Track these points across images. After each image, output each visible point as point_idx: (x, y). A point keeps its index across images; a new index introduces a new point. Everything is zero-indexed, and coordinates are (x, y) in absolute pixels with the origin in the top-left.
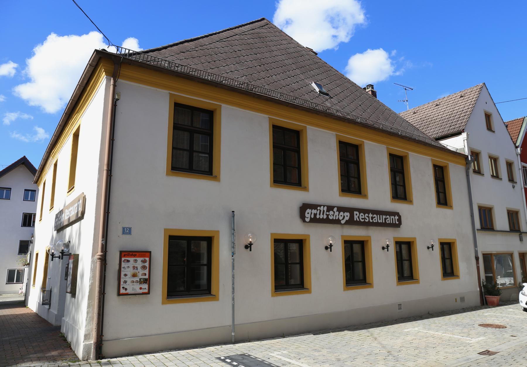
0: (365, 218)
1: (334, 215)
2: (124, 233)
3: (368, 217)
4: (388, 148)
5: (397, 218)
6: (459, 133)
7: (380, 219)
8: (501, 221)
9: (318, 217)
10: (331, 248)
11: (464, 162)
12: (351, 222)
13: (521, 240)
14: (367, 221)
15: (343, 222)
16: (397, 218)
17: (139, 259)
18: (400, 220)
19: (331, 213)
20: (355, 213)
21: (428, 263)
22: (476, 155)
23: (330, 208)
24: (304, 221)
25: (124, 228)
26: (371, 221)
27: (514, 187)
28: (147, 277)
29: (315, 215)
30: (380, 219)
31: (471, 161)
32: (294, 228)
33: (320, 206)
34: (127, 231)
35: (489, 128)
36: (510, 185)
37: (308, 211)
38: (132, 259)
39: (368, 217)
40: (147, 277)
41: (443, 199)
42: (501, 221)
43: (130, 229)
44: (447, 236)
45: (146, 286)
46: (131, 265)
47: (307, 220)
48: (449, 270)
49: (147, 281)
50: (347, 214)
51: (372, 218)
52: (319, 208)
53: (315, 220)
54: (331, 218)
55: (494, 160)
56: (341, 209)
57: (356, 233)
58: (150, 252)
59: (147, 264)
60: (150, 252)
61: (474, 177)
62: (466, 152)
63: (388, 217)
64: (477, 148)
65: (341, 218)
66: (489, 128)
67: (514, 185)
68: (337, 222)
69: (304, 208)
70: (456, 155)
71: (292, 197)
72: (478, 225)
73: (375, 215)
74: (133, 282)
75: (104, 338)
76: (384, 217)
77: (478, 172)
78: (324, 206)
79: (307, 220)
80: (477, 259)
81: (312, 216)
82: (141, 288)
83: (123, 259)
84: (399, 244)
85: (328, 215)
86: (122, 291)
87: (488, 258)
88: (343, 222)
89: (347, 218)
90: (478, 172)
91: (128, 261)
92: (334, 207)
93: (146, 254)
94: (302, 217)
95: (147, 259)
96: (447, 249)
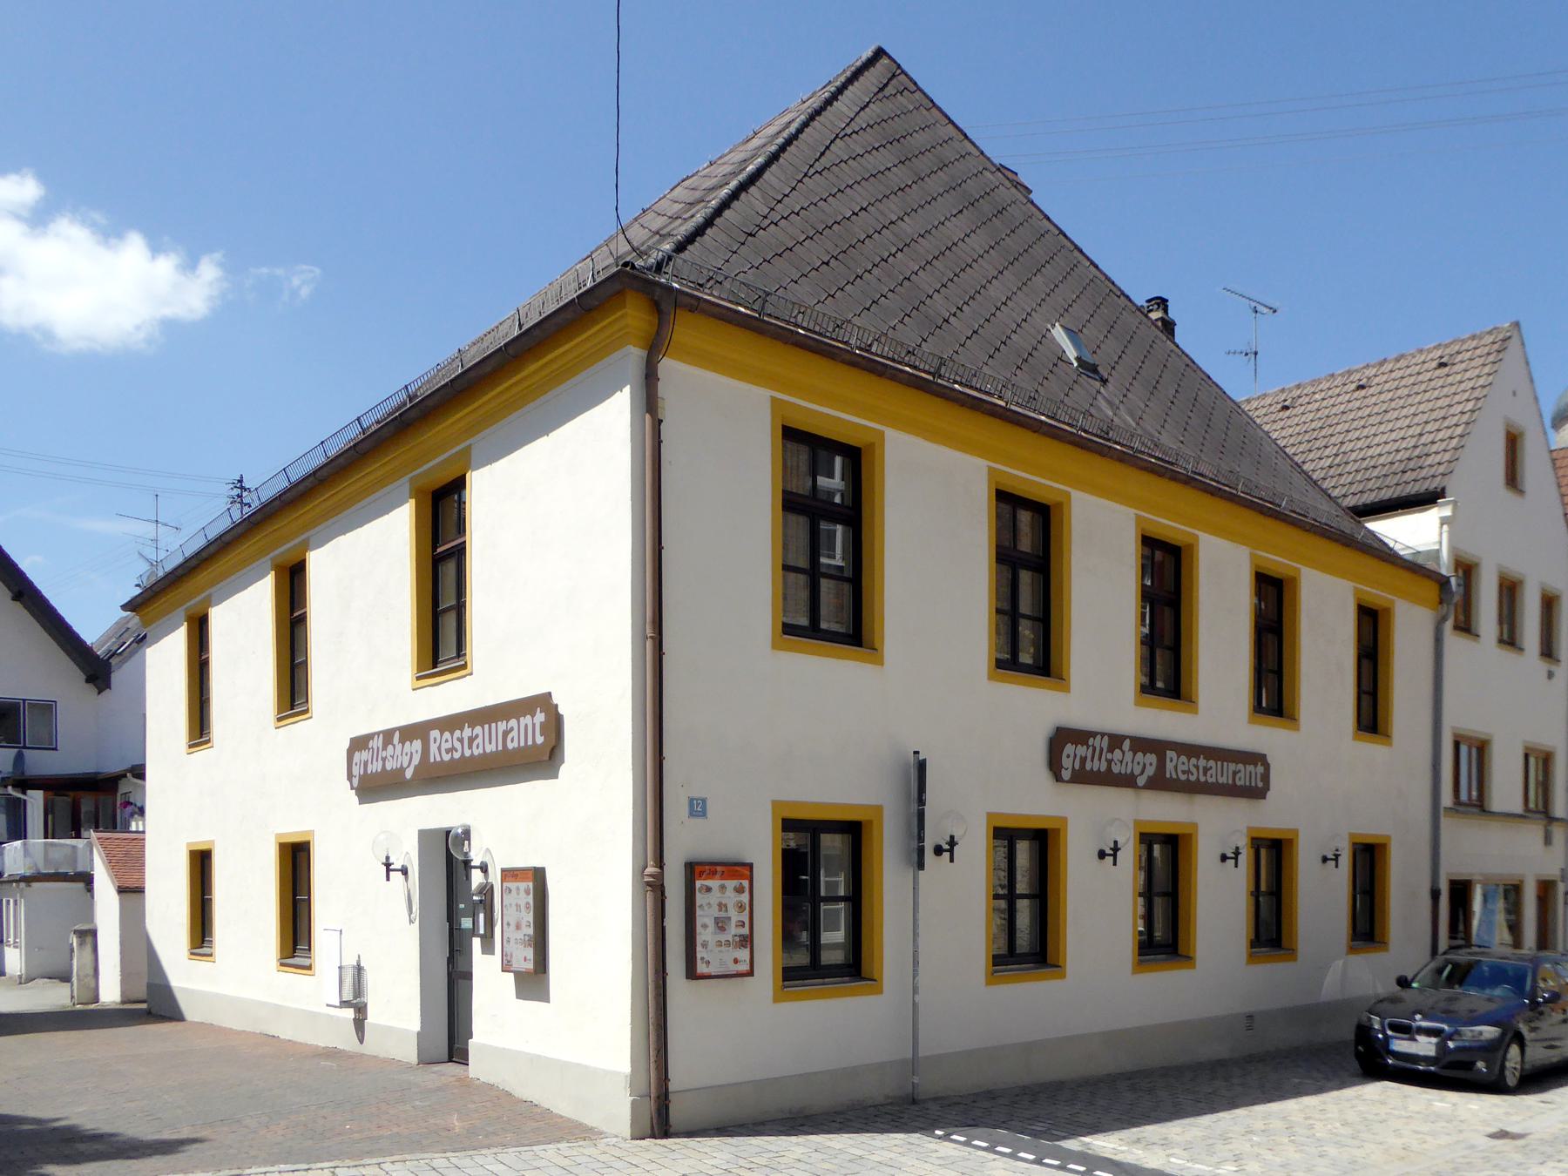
0: (1188, 772)
1: (1124, 762)
2: (693, 813)
3: (1197, 767)
4: (1252, 556)
5: (1260, 769)
6: (1426, 500)
7: (1220, 773)
8: (1506, 789)
9: (1088, 766)
10: (1115, 856)
11: (1431, 590)
12: (1160, 783)
13: (1548, 840)
14: (1193, 778)
15: (1141, 781)
16: (1260, 769)
17: (731, 884)
18: (1266, 777)
19: (1117, 754)
20: (1170, 754)
21: (1320, 895)
22: (1467, 570)
23: (1116, 741)
24: (1058, 778)
25: (691, 800)
26: (1202, 779)
27: (1550, 675)
28: (746, 931)
29: (1083, 760)
30: (1220, 773)
31: (1451, 590)
32: (1036, 798)
33: (1093, 734)
34: (698, 808)
35: (1513, 479)
36: (1542, 666)
37: (1069, 749)
38: (714, 883)
39: (1197, 767)
40: (746, 931)
41: (1371, 717)
42: (1506, 789)
43: (704, 801)
44: (1370, 829)
45: (744, 954)
46: (716, 896)
47: (1066, 775)
48: (1367, 926)
49: (747, 941)
50: (1152, 758)
51: (1206, 770)
52: (1091, 741)
53: (1083, 777)
54: (1116, 769)
55: (1510, 590)
56: (1142, 745)
57: (1166, 811)
58: (750, 866)
59: (745, 898)
60: (750, 866)
61: (1454, 643)
62: (1445, 568)
63: (1240, 766)
64: (1471, 550)
65: (1137, 771)
66: (1513, 479)
67: (1554, 668)
68: (1127, 781)
69: (1061, 738)
70: (1414, 569)
71: (1035, 708)
72: (1447, 799)
73: (1212, 763)
74: (719, 943)
75: (671, 1088)
76: (1232, 767)
77: (1466, 627)
78: (1103, 735)
79: (1066, 775)
80: (1435, 895)
81: (1077, 767)
82: (736, 961)
83: (698, 883)
84: (1257, 843)
85: (1109, 762)
86: (701, 968)
87: (1461, 892)
88: (1141, 781)
89: (1150, 771)
90: (1466, 627)
91: (709, 889)
92: (1124, 738)
93: (739, 870)
94: (1054, 765)
95: (746, 883)
96: (1369, 859)
